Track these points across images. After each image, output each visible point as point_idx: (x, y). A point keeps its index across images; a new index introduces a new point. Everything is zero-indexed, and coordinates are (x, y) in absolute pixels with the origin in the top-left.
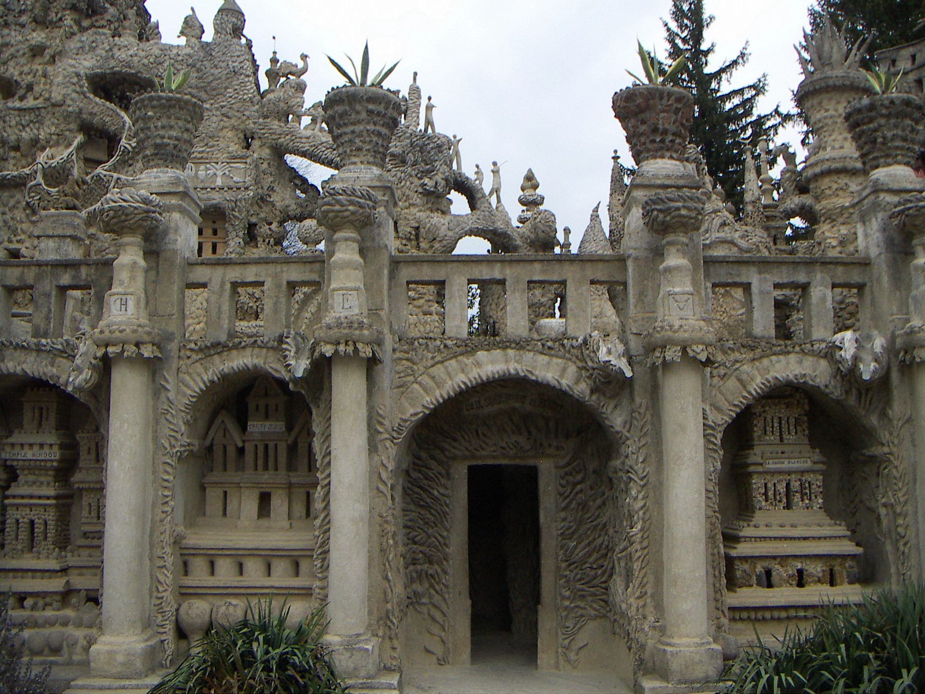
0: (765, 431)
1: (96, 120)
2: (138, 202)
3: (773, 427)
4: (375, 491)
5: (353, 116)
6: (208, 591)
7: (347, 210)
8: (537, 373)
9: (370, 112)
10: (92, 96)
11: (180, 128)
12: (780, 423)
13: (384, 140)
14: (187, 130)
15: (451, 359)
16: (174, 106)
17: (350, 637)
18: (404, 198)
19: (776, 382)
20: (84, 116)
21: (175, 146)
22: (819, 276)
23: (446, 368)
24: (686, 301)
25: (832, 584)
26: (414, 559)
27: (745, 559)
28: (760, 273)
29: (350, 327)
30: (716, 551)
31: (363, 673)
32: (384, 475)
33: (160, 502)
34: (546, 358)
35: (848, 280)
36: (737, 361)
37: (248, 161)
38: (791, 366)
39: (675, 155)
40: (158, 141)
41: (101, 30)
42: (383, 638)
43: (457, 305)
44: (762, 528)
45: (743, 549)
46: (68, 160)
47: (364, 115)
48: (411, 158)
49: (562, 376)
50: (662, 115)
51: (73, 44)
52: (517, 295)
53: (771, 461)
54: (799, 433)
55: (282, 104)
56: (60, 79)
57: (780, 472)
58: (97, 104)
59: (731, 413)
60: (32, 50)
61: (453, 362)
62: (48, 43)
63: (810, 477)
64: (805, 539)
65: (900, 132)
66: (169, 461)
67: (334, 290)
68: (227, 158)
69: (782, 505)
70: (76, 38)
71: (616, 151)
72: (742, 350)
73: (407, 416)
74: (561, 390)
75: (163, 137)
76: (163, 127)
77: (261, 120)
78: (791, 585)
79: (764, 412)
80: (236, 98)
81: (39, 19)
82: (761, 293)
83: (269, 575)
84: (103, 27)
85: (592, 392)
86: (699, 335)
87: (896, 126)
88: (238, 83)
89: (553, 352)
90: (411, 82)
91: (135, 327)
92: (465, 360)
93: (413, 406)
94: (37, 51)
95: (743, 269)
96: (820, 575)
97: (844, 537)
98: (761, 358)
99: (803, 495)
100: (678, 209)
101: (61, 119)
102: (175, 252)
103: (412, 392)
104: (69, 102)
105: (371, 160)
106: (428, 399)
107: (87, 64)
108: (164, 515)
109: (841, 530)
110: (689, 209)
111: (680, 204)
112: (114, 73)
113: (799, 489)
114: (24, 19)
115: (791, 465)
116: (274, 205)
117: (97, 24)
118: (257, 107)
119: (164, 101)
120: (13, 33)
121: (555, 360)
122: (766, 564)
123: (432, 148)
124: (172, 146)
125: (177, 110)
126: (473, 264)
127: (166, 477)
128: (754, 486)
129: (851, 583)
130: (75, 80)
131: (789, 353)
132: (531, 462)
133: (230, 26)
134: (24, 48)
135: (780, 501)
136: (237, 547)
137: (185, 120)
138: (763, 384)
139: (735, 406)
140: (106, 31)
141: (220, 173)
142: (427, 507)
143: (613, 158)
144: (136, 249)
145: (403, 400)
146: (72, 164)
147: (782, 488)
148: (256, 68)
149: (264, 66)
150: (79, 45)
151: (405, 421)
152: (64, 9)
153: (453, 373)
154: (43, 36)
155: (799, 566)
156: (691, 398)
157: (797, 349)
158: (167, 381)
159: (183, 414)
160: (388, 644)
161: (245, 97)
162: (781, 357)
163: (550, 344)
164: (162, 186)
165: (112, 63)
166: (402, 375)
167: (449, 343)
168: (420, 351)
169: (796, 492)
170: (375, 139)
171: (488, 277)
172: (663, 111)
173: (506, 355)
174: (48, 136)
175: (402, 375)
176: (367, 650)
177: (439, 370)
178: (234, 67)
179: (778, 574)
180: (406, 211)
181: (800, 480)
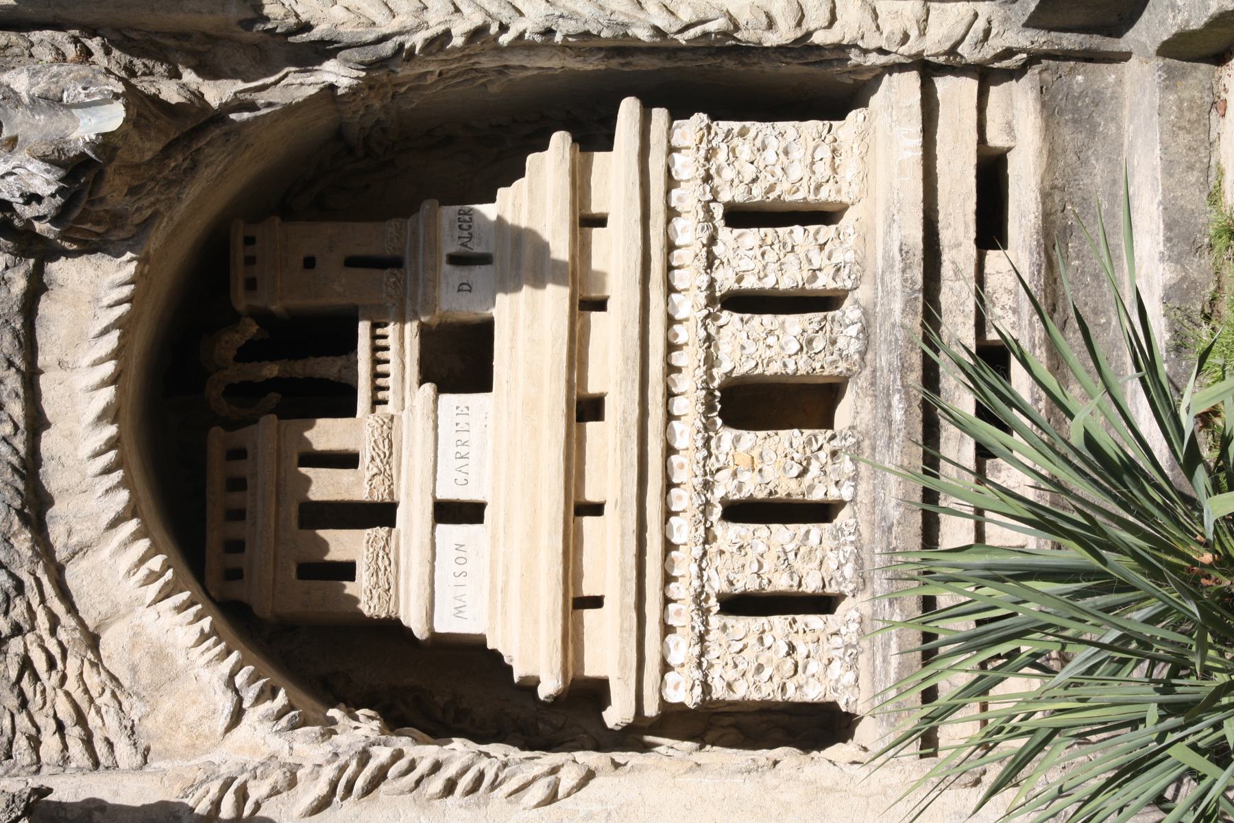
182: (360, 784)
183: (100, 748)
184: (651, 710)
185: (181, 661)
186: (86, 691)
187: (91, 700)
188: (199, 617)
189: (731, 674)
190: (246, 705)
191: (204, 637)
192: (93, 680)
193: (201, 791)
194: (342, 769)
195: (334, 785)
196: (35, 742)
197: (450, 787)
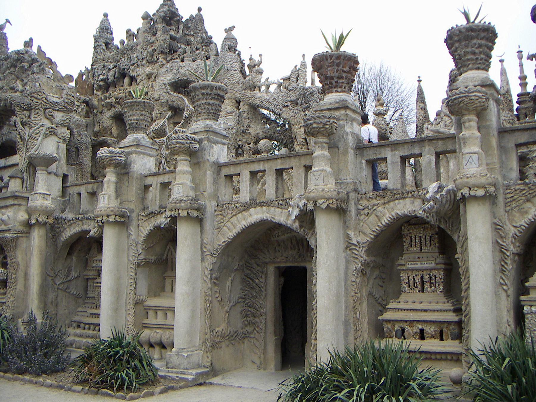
0: (411, 245)
1: (174, 104)
2: (107, 153)
3: (416, 242)
4: (203, 281)
5: (197, 97)
6: (154, 326)
7: (176, 147)
8: (276, 218)
9: (203, 94)
10: (172, 93)
11: (138, 114)
12: (421, 240)
13: (212, 106)
14: (142, 115)
15: (239, 213)
16: (134, 105)
17: (179, 349)
18: (298, 124)
19: (398, 216)
20: (169, 103)
21: (137, 123)
22: (427, 148)
23: (237, 218)
24: (320, 175)
25: (442, 339)
26: (246, 315)
27: (389, 321)
28: (392, 151)
29: (175, 203)
30: (355, 316)
31: (182, 367)
32: (206, 273)
33: (129, 285)
34: (280, 210)
35: (445, 149)
36: (374, 205)
37: (234, 114)
38: (407, 206)
39: (339, 90)
40: (130, 122)
41: (175, 60)
42: (204, 351)
43: (245, 185)
44: (402, 303)
45: (387, 316)
46: (163, 125)
47: (201, 96)
48: (300, 101)
49: (287, 219)
50: (329, 69)
51: (163, 70)
52: (270, 177)
53: (410, 263)
54: (432, 246)
55: (251, 82)
56: (157, 88)
57: (417, 270)
58: (175, 96)
59: (371, 236)
60: (147, 76)
61: (240, 215)
62: (153, 72)
63: (435, 273)
64: (426, 311)
65: (469, 50)
66: (132, 267)
67: (174, 185)
68: (225, 114)
69: (417, 290)
70: (165, 66)
71: (419, 77)
72: (378, 198)
73: (221, 243)
74: (287, 226)
75: (131, 120)
76: (131, 116)
77: (243, 92)
78: (415, 338)
79: (410, 233)
80: (229, 83)
81: (150, 61)
82: (392, 163)
83: (167, 319)
84: (176, 58)
85: (301, 227)
86: (321, 194)
87: (467, 46)
88: (229, 75)
89: (283, 207)
90: (302, 59)
91: (106, 209)
92: (245, 213)
93: (224, 238)
94: (149, 76)
95: (382, 150)
96: (433, 333)
97: (450, 310)
98: (389, 202)
99: (431, 283)
100: (311, 124)
101: (160, 106)
102: (133, 172)
103: (223, 231)
104: (162, 98)
105: (207, 117)
106: (230, 234)
107: (168, 78)
108: (131, 291)
109: (449, 306)
110: (318, 123)
111: (312, 122)
112: (180, 80)
113: (428, 280)
114: (144, 62)
115: (422, 265)
116: (250, 134)
117: (173, 58)
118: (241, 85)
119: (129, 104)
120: (141, 70)
121: (284, 211)
122: (400, 325)
123: (308, 95)
124: (135, 123)
125: (135, 107)
126: (251, 164)
127: (131, 274)
128: (401, 278)
129: (452, 339)
130: (164, 87)
131: (405, 198)
132: (303, 264)
133: (227, 47)
134: (144, 76)
135: (416, 287)
136: (163, 306)
137: (140, 110)
138: (390, 218)
139: (374, 231)
140: (177, 60)
141: (222, 122)
142: (253, 288)
143: (418, 81)
144: (111, 173)
145: (219, 235)
146: (165, 126)
147: (418, 280)
148: (243, 65)
149: (247, 62)
150: (166, 69)
151: (220, 245)
152: (159, 54)
153: (240, 220)
154: (151, 68)
155: (420, 327)
156: (324, 229)
157: (410, 195)
158: (132, 231)
159: (141, 245)
160: (205, 355)
161: (234, 81)
162: (401, 201)
163: (280, 202)
164: (129, 143)
165: (178, 76)
166: (219, 222)
167: (238, 205)
168: (226, 210)
169: (427, 282)
170: (207, 107)
171: (258, 170)
172: (330, 66)
173: (263, 209)
174: (156, 115)
175: (219, 222)
176: (184, 356)
177: (234, 219)
178: (227, 68)
179: (407, 331)
180: (299, 130)
181: (429, 274)
182: (503, 250)
183: (509, 204)
184: (522, 303)
185: (526, 216)
186: (519, 200)
187: (517, 202)
188: (534, 218)
189: (530, 318)
190: (518, 229)
191: (530, 220)
192: (521, 201)
193: (500, 222)
194: (505, 246)
195: (502, 245)
196: (509, 193)
197: (503, 266)
